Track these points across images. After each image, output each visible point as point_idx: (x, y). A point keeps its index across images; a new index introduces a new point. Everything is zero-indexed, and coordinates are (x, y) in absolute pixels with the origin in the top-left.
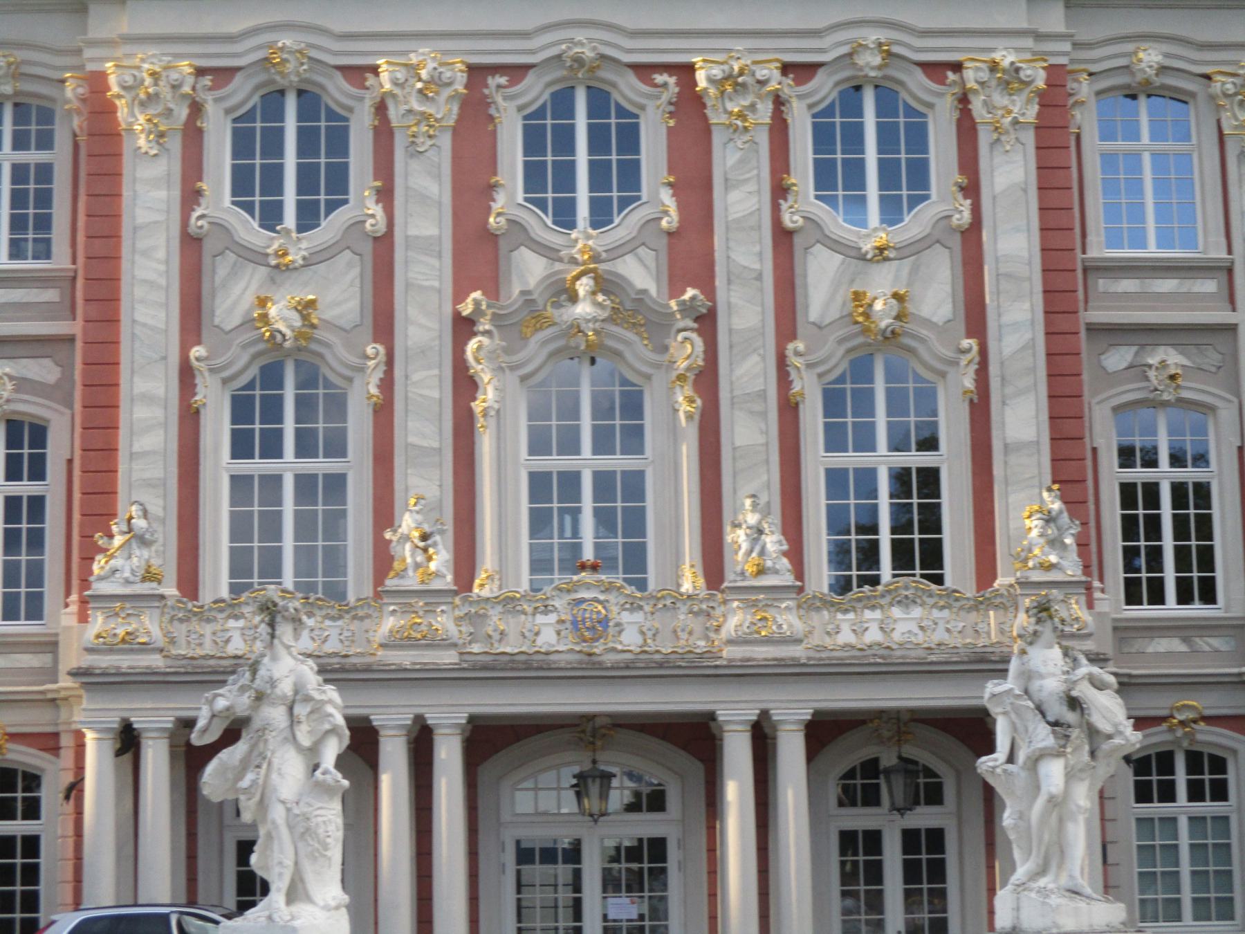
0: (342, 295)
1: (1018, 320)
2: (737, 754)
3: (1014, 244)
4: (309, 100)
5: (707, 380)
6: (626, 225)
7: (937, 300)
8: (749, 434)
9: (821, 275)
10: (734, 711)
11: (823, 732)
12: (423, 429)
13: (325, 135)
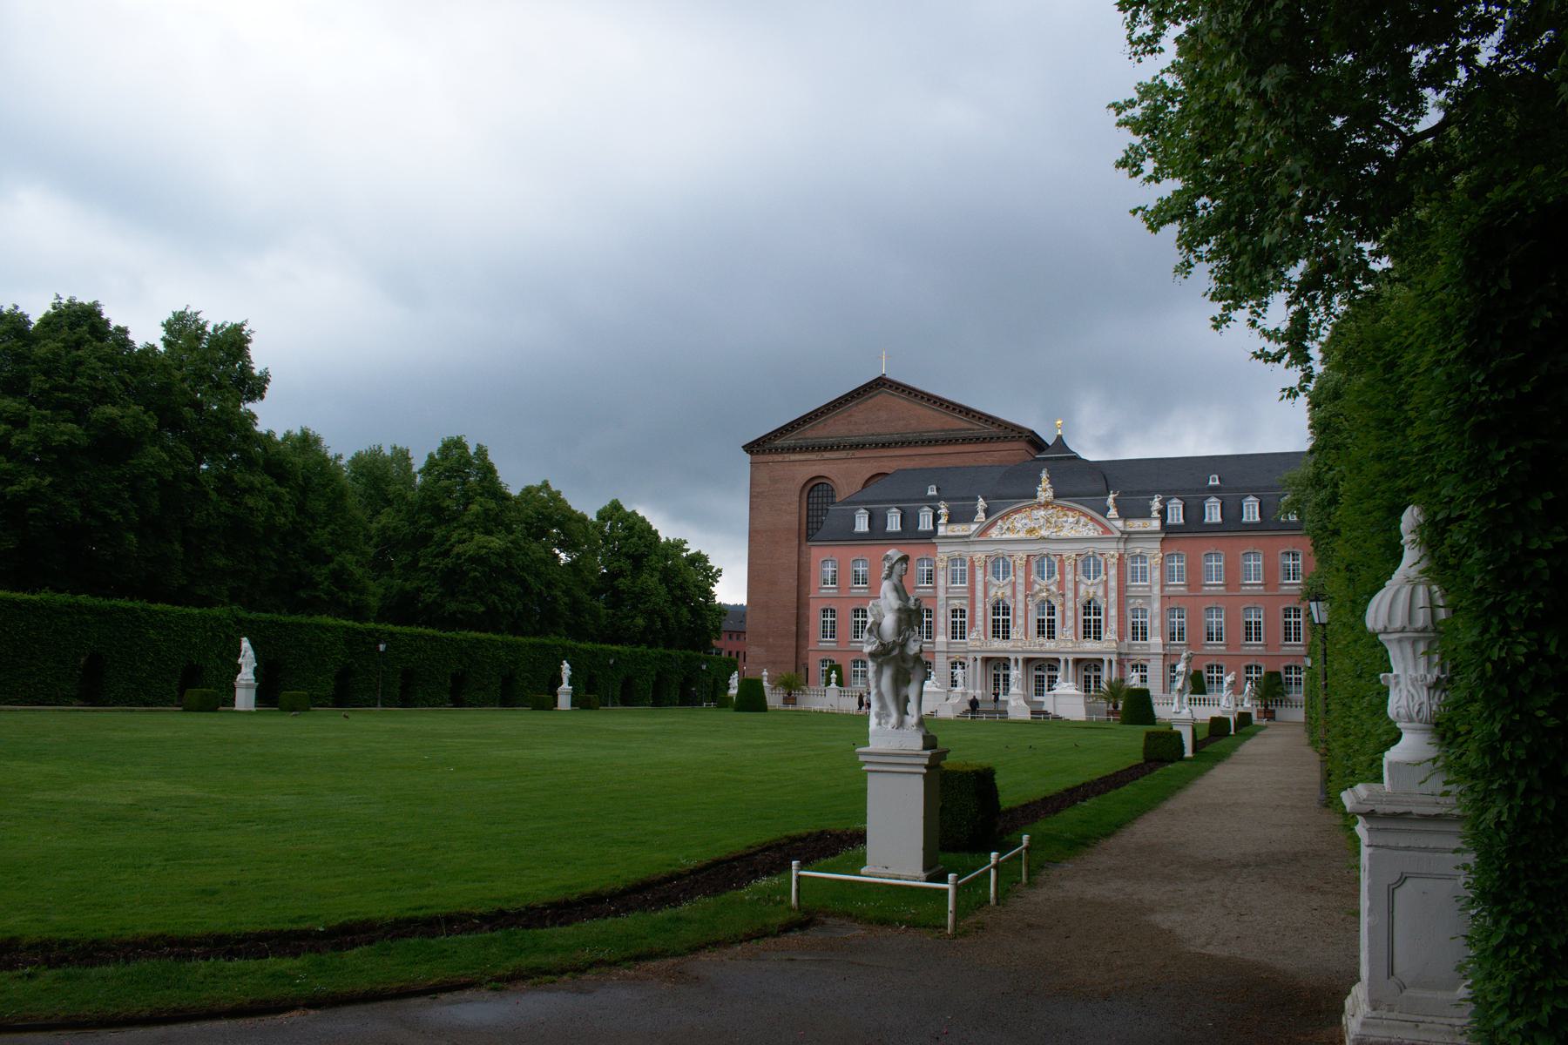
0: (1008, 592)
1: (1113, 596)
3: (1113, 584)
5: (1063, 605)
7: (1100, 593)
8: (1070, 614)
9: (1082, 588)
10: (1062, 658)
12: (1020, 613)
13: (1006, 566)
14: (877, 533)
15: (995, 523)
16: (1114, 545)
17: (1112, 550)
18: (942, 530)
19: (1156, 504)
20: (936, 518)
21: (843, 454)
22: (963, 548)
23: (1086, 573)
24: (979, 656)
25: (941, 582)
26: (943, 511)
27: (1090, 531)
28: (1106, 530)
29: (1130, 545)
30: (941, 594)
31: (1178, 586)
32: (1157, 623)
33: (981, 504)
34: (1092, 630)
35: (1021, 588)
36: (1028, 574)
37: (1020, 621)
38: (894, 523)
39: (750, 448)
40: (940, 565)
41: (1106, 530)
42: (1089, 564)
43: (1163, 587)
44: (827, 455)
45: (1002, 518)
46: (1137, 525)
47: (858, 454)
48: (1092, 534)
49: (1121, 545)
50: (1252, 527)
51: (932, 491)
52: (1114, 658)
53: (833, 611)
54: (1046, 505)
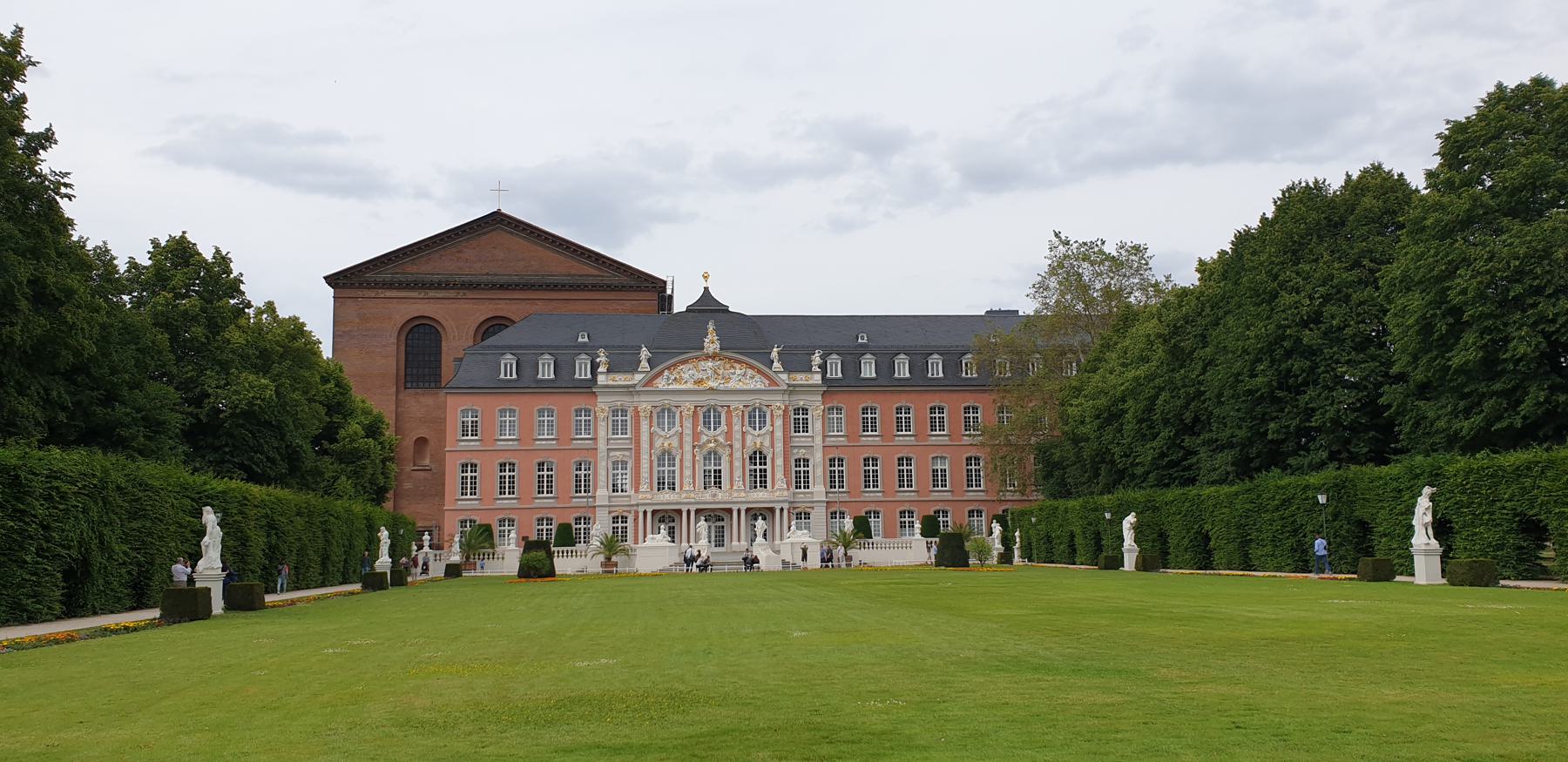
1: (779, 446)
2: (735, 514)
3: (779, 434)
4: (669, 410)
5: (731, 455)
6: (719, 431)
7: (767, 443)
8: (738, 464)
9: (749, 439)
10: (735, 508)
11: (748, 510)
12: (688, 464)
14: (526, 384)
15: (660, 373)
16: (779, 397)
17: (778, 402)
18: (601, 379)
19: (817, 359)
20: (594, 366)
21: (452, 293)
22: (627, 399)
23: (752, 424)
24: (649, 510)
25: (602, 433)
26: (602, 358)
27: (758, 383)
28: (773, 382)
29: (794, 398)
30: (602, 446)
31: (838, 438)
32: (819, 472)
33: (645, 353)
34: (759, 480)
35: (688, 439)
36: (695, 426)
37: (688, 472)
38: (546, 372)
39: (332, 280)
40: (601, 416)
41: (773, 382)
42: (756, 417)
43: (824, 437)
44: (432, 294)
45: (668, 368)
46: (800, 378)
47: (469, 294)
48: (759, 386)
49: (786, 397)
50: (903, 382)
51: (583, 339)
52: (785, 506)
53: (474, 466)
54: (713, 357)
